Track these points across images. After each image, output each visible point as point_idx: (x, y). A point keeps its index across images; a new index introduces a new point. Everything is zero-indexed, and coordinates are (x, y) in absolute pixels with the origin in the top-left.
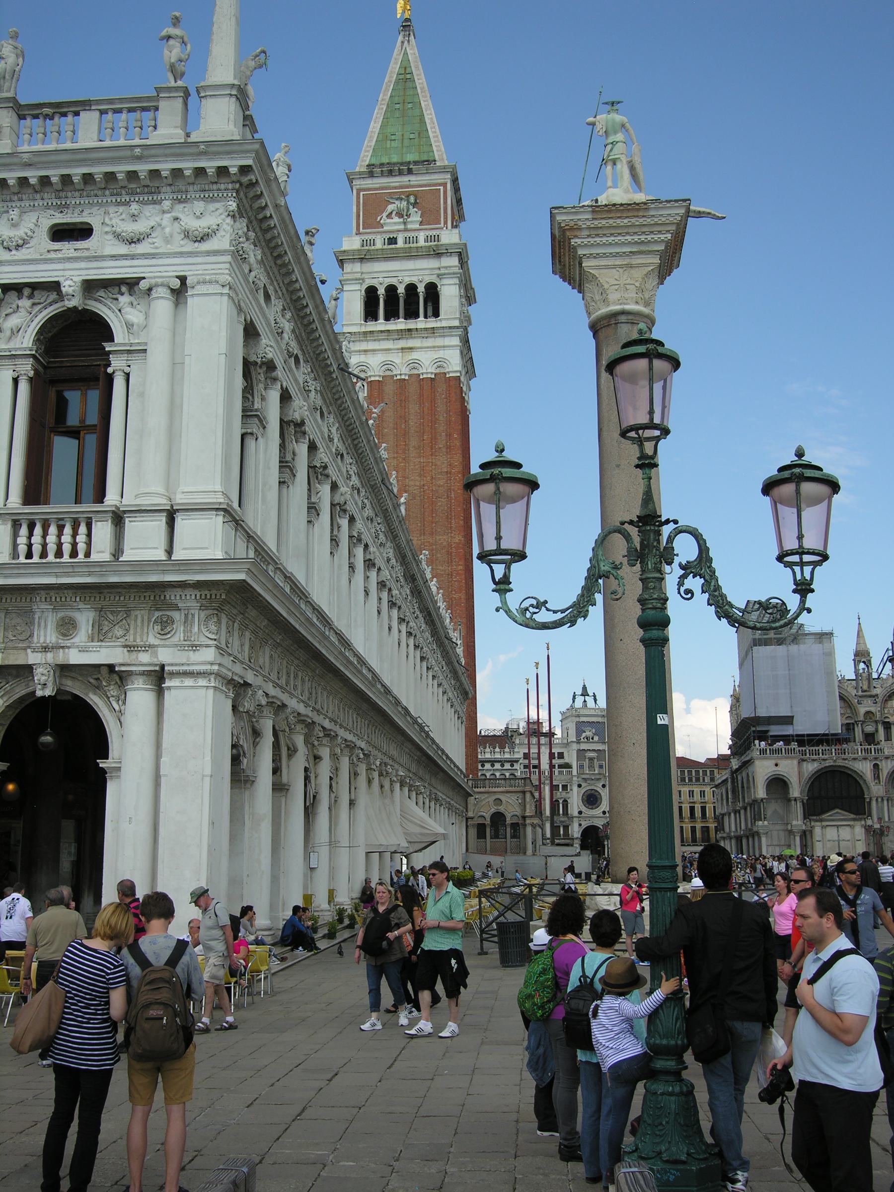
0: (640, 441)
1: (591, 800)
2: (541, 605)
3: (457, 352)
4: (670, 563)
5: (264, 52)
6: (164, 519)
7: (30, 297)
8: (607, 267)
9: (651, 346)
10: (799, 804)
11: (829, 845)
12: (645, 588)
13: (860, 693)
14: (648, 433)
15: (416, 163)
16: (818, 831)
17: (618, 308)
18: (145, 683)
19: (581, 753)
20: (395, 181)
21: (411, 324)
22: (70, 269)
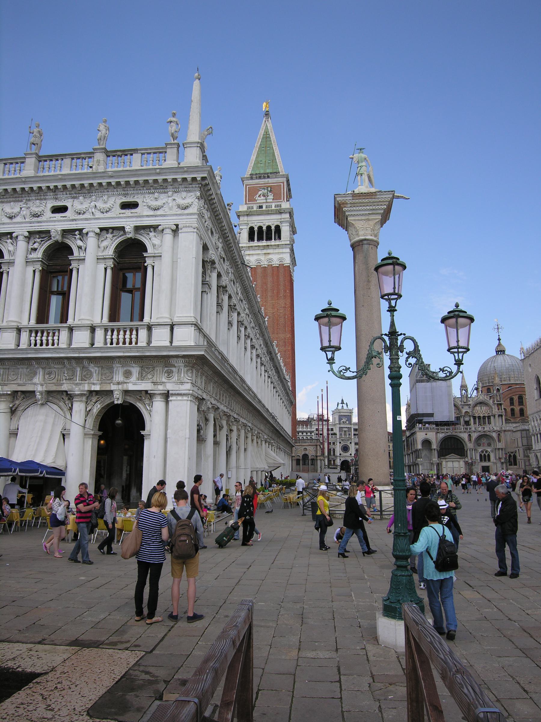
0: (389, 300)
1: (345, 449)
2: (347, 369)
4: (402, 352)
7: (112, 233)
8: (358, 220)
9: (394, 260)
10: (436, 452)
11: (449, 469)
12: (391, 363)
13: (463, 403)
14: (393, 297)
15: (271, 173)
16: (444, 463)
17: (363, 238)
19: (341, 429)
21: (269, 243)
22: (129, 221)
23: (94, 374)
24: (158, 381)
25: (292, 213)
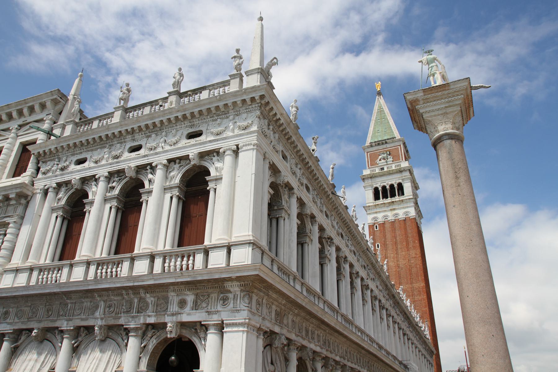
3: (413, 208)
5: (275, 58)
6: (226, 250)
7: (179, 163)
8: (435, 116)
15: (388, 139)
18: (215, 330)
20: (381, 147)
21: (393, 199)
23: (150, 305)
24: (213, 310)
25: (411, 170)
